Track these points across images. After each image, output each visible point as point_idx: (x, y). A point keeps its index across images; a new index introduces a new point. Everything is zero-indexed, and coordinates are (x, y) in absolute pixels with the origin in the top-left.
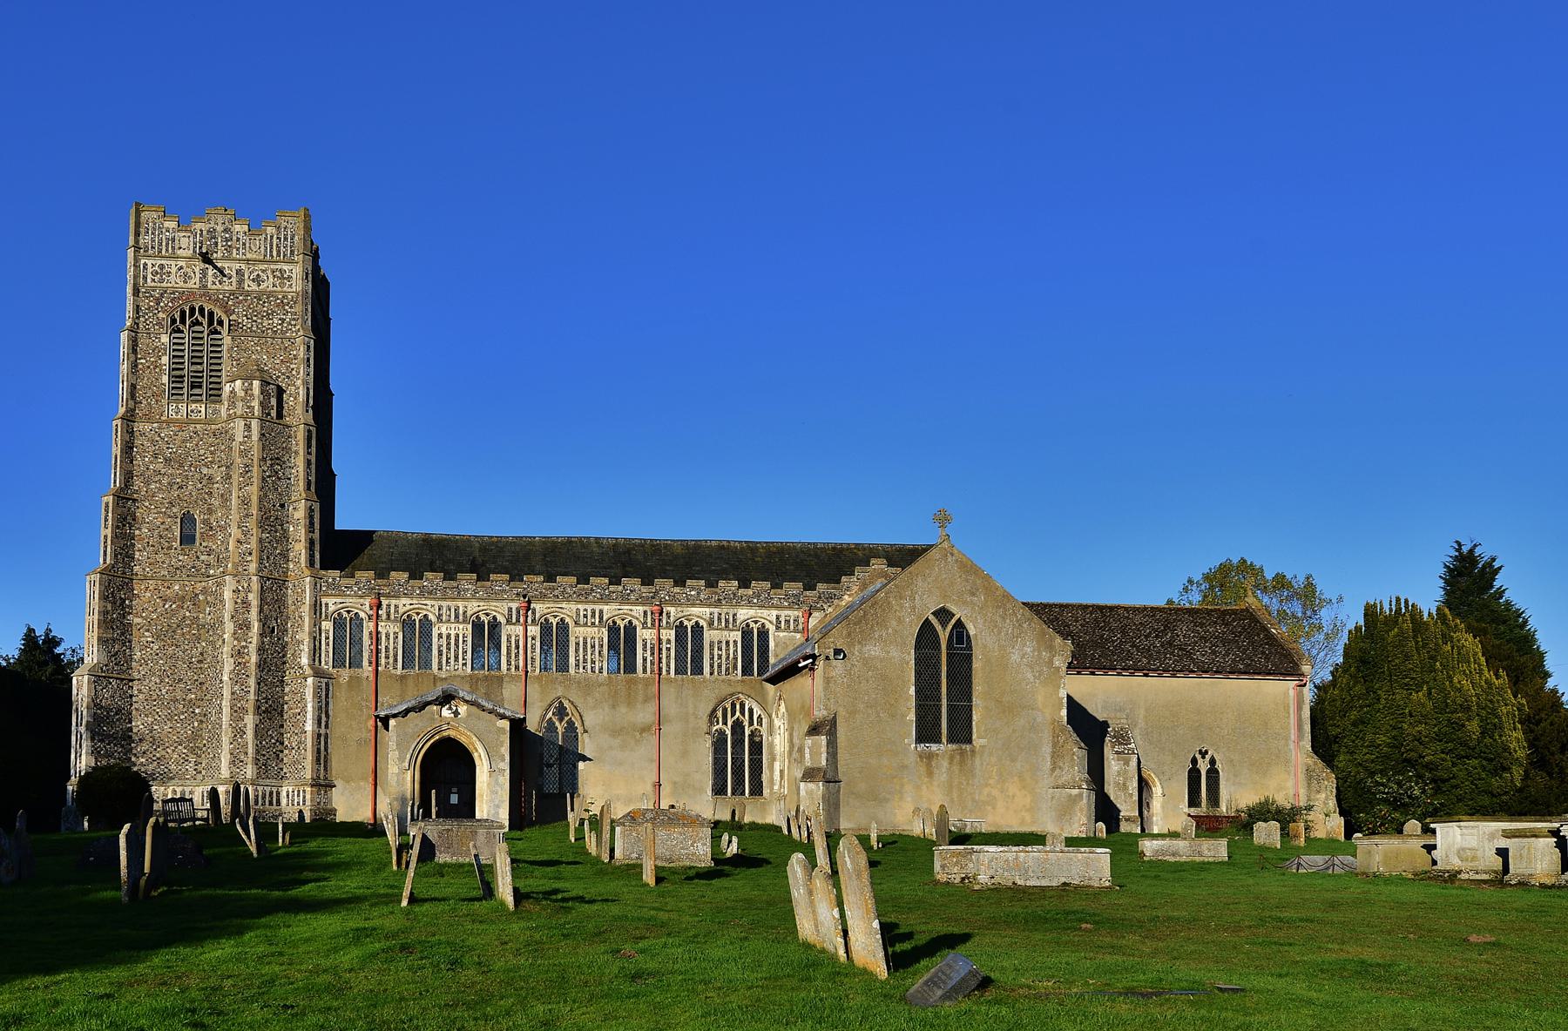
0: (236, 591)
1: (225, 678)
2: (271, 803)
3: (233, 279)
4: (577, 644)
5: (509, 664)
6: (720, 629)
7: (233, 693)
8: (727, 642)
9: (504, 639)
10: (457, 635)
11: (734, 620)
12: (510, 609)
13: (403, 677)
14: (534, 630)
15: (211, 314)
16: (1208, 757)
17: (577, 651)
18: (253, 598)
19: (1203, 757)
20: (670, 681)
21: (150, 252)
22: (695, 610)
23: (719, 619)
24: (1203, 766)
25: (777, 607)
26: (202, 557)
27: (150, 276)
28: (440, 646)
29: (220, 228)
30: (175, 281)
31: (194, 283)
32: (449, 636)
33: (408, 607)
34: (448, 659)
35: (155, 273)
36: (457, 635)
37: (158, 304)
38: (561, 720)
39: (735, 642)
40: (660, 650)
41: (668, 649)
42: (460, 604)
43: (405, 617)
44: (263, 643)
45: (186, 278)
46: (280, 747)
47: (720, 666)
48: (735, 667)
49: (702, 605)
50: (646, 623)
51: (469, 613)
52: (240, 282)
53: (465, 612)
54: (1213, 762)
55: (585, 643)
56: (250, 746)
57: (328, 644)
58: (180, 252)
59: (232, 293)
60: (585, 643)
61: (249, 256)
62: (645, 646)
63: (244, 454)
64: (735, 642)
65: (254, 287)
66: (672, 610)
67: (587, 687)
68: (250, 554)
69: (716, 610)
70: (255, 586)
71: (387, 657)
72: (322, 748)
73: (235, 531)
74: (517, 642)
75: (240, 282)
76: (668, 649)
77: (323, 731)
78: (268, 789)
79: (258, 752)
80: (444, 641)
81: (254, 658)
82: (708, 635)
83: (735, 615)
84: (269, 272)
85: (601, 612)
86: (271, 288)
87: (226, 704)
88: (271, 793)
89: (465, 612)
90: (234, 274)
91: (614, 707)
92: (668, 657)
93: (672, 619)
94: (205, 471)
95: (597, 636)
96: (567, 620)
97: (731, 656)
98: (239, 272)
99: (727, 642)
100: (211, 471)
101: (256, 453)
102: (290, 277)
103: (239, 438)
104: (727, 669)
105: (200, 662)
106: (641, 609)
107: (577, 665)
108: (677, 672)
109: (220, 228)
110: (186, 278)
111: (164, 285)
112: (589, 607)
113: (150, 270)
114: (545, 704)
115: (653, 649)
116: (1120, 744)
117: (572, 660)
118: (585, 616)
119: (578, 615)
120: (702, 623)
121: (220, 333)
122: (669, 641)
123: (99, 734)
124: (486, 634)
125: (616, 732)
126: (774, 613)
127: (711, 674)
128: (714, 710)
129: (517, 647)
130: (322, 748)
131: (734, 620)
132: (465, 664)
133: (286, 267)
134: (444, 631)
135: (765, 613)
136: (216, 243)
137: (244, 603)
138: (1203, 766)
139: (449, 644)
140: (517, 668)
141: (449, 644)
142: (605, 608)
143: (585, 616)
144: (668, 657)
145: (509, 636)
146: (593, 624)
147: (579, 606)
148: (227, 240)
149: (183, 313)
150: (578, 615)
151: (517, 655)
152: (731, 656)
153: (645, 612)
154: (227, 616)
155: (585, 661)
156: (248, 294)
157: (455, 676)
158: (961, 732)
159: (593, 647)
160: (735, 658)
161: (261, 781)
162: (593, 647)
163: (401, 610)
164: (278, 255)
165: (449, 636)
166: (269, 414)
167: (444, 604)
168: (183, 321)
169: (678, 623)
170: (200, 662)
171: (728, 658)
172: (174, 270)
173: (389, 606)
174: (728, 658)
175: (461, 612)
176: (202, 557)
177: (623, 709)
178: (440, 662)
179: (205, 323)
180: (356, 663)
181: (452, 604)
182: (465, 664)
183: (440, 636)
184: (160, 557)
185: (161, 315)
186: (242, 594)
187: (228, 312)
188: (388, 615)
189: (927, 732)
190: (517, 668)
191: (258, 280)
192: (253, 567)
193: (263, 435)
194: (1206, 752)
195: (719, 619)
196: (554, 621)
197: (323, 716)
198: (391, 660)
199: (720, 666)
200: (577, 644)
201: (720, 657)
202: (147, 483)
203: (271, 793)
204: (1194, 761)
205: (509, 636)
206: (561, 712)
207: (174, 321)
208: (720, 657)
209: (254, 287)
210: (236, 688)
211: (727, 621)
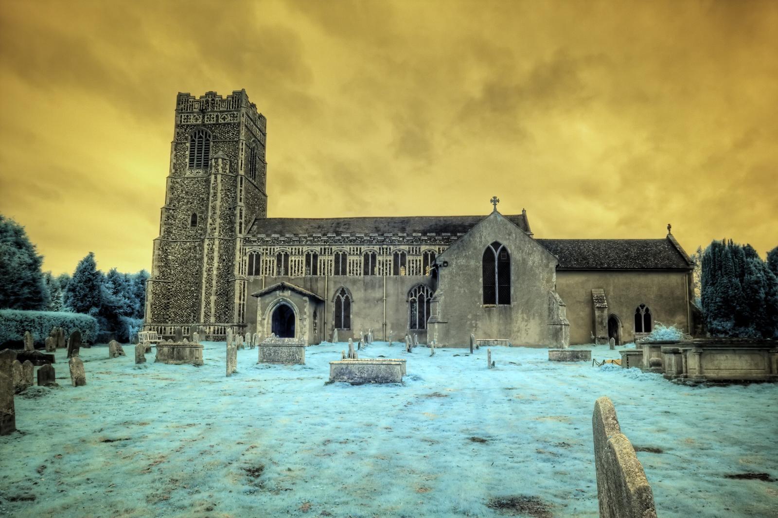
0: (209, 245)
1: (203, 281)
2: (221, 333)
3: (215, 119)
4: (350, 263)
5: (320, 272)
6: (413, 255)
7: (206, 287)
8: (416, 261)
9: (319, 261)
10: (299, 261)
11: (419, 251)
12: (321, 249)
13: (275, 279)
14: (333, 258)
15: (206, 133)
16: (645, 308)
17: (350, 266)
18: (216, 249)
19: (642, 309)
20: (390, 278)
21: (184, 111)
22: (402, 247)
23: (413, 250)
24: (643, 313)
25: (439, 245)
26: (199, 231)
27: (183, 120)
28: (292, 265)
29: (210, 99)
30: (192, 121)
31: (199, 122)
32: (295, 261)
33: (279, 249)
34: (295, 271)
35: (185, 119)
36: (299, 261)
37: (185, 131)
38: (343, 296)
39: (420, 260)
40: (386, 265)
41: (390, 264)
42: (301, 247)
43: (277, 253)
44: (219, 266)
45: (197, 119)
46: (227, 310)
47: (413, 271)
48: (420, 272)
49: (404, 245)
50: (380, 253)
51: (304, 251)
52: (217, 120)
53: (302, 251)
54: (647, 310)
55: (353, 262)
56: (212, 309)
57: (245, 266)
58: (194, 110)
59: (214, 124)
60: (353, 262)
61: (221, 109)
62: (380, 263)
63: (214, 188)
64: (420, 260)
65: (223, 121)
66: (392, 247)
67: (354, 282)
68: (215, 229)
69: (411, 247)
70: (217, 242)
71: (270, 270)
72: (241, 310)
73: (210, 221)
74: (324, 263)
75: (217, 120)
76: (390, 264)
77: (242, 302)
78: (220, 327)
79: (216, 312)
80: (293, 263)
81: (215, 272)
82: (408, 258)
83: (420, 248)
84: (229, 116)
85: (360, 249)
86: (229, 121)
87: (203, 292)
88: (221, 329)
89: (302, 251)
90: (215, 117)
91: (365, 290)
92: (390, 268)
93: (392, 251)
94: (201, 196)
95: (358, 259)
96: (346, 253)
97: (418, 266)
98: (217, 116)
99: (416, 261)
100: (203, 196)
101: (220, 187)
102: (237, 116)
103: (212, 182)
104: (416, 272)
105: (196, 274)
106: (378, 247)
107: (350, 272)
108: (394, 274)
109: (210, 99)
110: (197, 119)
111: (188, 123)
112: (355, 247)
113: (183, 117)
114: (336, 289)
115: (383, 264)
116: (599, 302)
117: (348, 270)
118: (354, 251)
119: (350, 250)
120: (405, 252)
121: (209, 140)
122: (390, 261)
123: (154, 304)
124: (312, 260)
125: (367, 301)
126: (437, 247)
127: (409, 274)
128: (410, 291)
129: (324, 265)
130: (241, 310)
131: (419, 251)
132: (302, 273)
133: (235, 113)
134: (293, 259)
135: (433, 247)
136: (208, 106)
137: (211, 249)
138: (643, 313)
139: (295, 264)
140: (324, 274)
141: (295, 264)
142: (362, 247)
143: (354, 251)
144: (390, 268)
145: (321, 260)
146: (357, 254)
147: (351, 247)
148: (213, 104)
149: (195, 133)
150: (350, 250)
151: (324, 268)
152: (418, 266)
153: (380, 248)
154: (205, 255)
155: (353, 270)
156: (220, 124)
157: (298, 278)
158: (506, 299)
159: (357, 264)
160: (420, 267)
161: (217, 324)
162: (357, 264)
163: (276, 250)
164: (233, 108)
165: (295, 261)
166: (225, 172)
167: (294, 247)
168: (195, 138)
169: (394, 253)
170: (196, 274)
171: (416, 267)
172: (192, 117)
173: (271, 249)
174: (416, 267)
175: (300, 250)
176: (199, 231)
177: (370, 291)
178: (291, 272)
179: (204, 137)
180: (257, 273)
181: (297, 247)
182: (302, 273)
183: (292, 261)
184: (183, 232)
185: (186, 135)
186: (211, 246)
187: (213, 132)
188: (270, 254)
189: (489, 298)
190: (324, 274)
191: (224, 119)
192: (216, 234)
193: (222, 180)
194: (644, 306)
195: (413, 250)
196: (341, 253)
197: (242, 296)
198: (271, 272)
199: (413, 271)
200: (350, 263)
201: (413, 267)
202: (179, 202)
203: (221, 329)
204: (638, 310)
205: (321, 260)
206: (343, 292)
207: (192, 137)
208: (413, 267)
209: (223, 121)
210: (208, 285)
211: (416, 251)
